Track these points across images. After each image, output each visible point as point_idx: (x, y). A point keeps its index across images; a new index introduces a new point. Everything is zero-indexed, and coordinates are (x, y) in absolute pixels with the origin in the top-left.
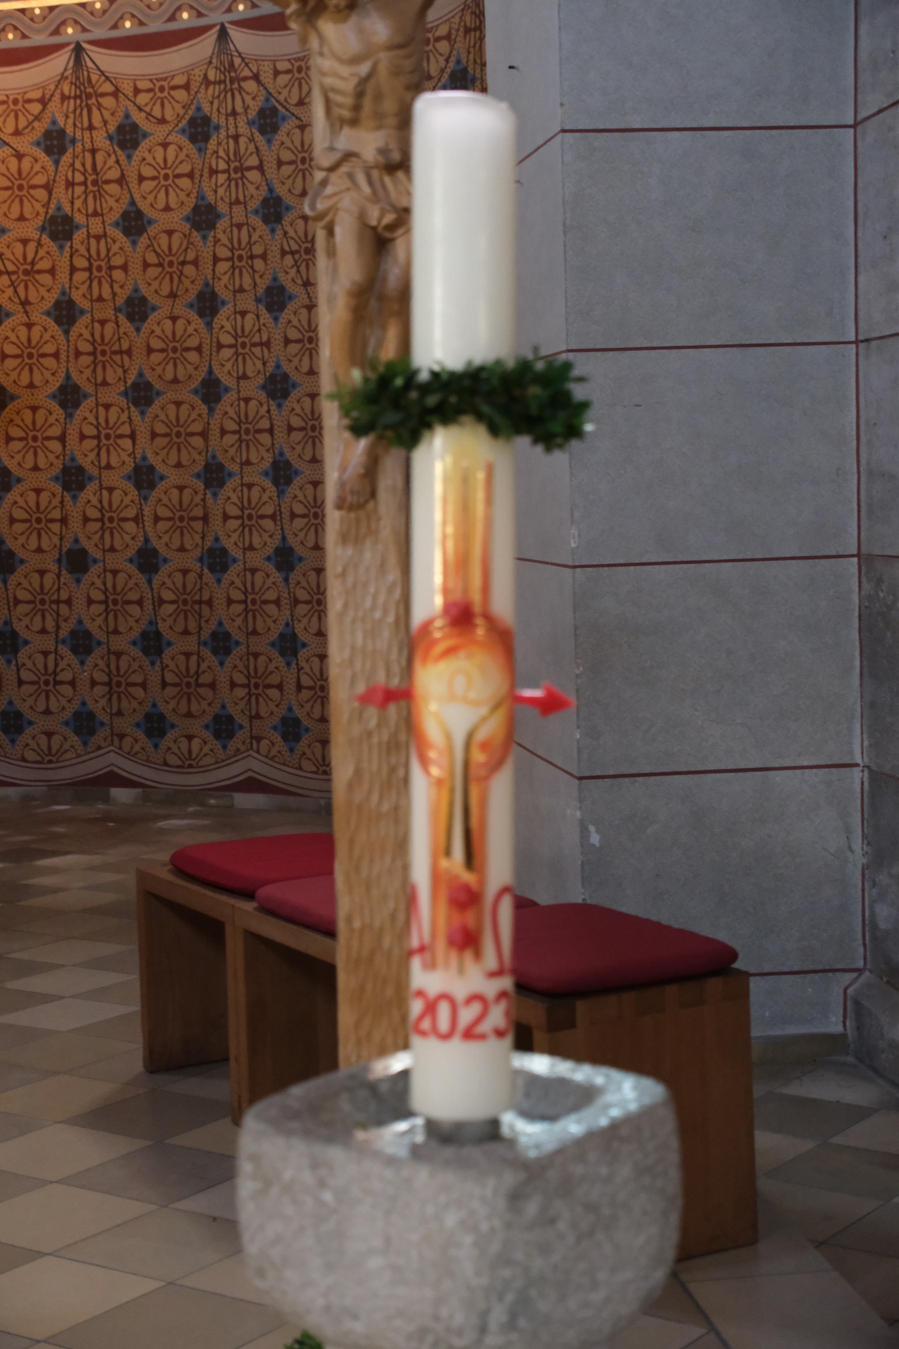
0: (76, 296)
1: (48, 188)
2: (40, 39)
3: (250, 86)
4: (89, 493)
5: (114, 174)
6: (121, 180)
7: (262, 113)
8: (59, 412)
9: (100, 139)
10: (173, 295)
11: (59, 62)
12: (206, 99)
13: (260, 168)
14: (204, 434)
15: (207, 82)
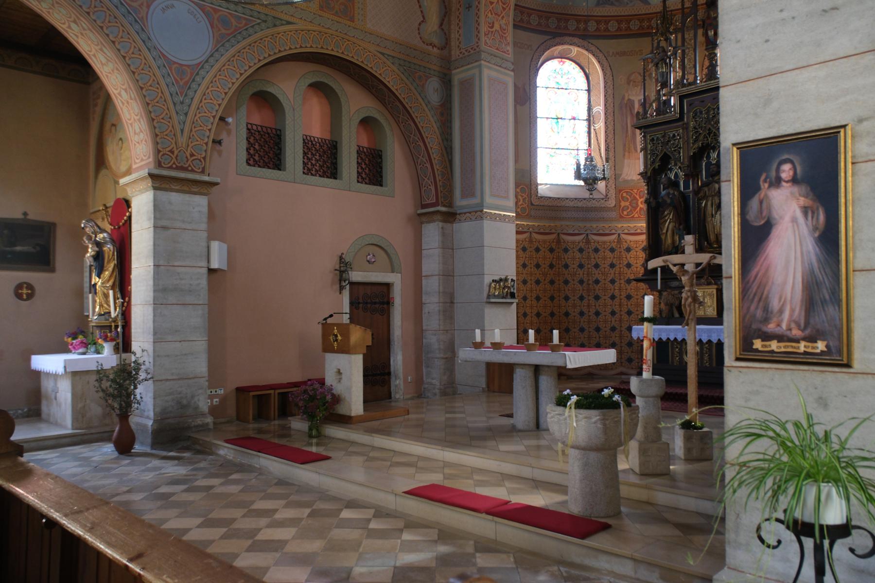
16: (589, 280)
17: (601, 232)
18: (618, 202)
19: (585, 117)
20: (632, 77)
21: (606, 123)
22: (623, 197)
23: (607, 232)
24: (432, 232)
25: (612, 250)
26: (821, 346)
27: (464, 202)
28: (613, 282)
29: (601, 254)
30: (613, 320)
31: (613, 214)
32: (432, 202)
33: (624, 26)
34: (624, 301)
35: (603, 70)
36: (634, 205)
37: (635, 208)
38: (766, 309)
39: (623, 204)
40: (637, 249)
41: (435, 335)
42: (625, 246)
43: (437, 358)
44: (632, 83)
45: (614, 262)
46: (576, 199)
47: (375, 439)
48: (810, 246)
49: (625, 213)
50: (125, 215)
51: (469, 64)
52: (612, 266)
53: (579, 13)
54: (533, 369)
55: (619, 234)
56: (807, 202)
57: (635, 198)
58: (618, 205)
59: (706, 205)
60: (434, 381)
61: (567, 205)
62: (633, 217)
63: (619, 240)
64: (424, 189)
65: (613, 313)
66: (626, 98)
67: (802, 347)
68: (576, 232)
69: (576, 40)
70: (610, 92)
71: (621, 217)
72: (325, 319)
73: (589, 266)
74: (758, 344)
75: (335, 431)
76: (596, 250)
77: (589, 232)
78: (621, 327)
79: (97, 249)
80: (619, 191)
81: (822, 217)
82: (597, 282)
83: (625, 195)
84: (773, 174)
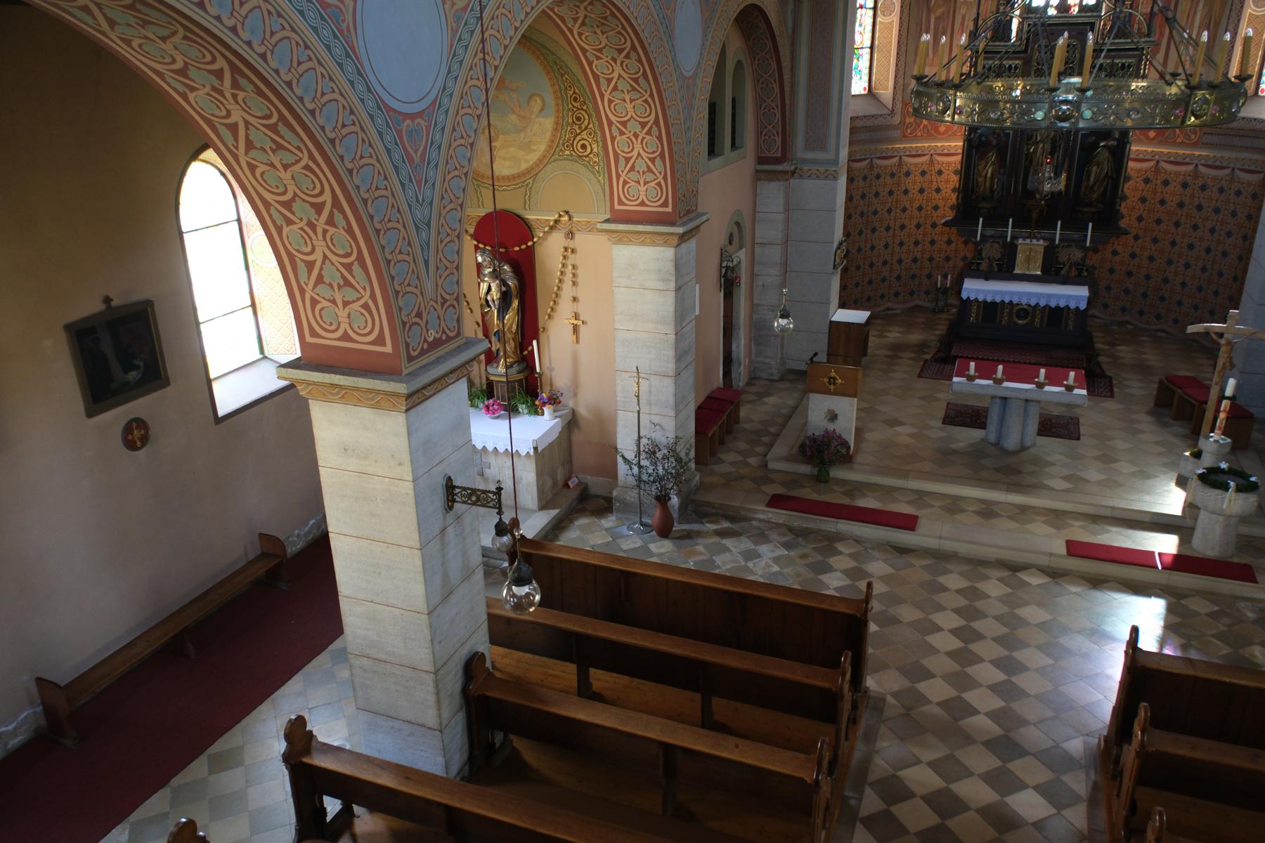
0: (1144, 216)
1: (1143, 191)
2: (1148, 157)
3: (1201, 179)
4: (1137, 260)
5: (1160, 190)
6: (1162, 192)
7: (1202, 186)
9: (1159, 182)
11: (1152, 164)
12: (1189, 179)
13: (1199, 198)
14: (1169, 253)
15: (1189, 175)
16: (868, 211)
17: (884, 155)
18: (903, 117)
21: (901, 18)
23: (890, 154)
24: (773, 193)
27: (809, 155)
28: (889, 211)
29: (882, 179)
30: (886, 252)
31: (897, 134)
37: (919, 125)
40: (916, 173)
41: (773, 311)
42: (905, 169)
46: (865, 117)
49: (909, 131)
52: (891, 193)
58: (903, 122)
59: (1035, 151)
60: (767, 360)
64: (763, 138)
68: (863, 157)
71: (905, 136)
72: (811, 359)
75: (838, 473)
76: (878, 177)
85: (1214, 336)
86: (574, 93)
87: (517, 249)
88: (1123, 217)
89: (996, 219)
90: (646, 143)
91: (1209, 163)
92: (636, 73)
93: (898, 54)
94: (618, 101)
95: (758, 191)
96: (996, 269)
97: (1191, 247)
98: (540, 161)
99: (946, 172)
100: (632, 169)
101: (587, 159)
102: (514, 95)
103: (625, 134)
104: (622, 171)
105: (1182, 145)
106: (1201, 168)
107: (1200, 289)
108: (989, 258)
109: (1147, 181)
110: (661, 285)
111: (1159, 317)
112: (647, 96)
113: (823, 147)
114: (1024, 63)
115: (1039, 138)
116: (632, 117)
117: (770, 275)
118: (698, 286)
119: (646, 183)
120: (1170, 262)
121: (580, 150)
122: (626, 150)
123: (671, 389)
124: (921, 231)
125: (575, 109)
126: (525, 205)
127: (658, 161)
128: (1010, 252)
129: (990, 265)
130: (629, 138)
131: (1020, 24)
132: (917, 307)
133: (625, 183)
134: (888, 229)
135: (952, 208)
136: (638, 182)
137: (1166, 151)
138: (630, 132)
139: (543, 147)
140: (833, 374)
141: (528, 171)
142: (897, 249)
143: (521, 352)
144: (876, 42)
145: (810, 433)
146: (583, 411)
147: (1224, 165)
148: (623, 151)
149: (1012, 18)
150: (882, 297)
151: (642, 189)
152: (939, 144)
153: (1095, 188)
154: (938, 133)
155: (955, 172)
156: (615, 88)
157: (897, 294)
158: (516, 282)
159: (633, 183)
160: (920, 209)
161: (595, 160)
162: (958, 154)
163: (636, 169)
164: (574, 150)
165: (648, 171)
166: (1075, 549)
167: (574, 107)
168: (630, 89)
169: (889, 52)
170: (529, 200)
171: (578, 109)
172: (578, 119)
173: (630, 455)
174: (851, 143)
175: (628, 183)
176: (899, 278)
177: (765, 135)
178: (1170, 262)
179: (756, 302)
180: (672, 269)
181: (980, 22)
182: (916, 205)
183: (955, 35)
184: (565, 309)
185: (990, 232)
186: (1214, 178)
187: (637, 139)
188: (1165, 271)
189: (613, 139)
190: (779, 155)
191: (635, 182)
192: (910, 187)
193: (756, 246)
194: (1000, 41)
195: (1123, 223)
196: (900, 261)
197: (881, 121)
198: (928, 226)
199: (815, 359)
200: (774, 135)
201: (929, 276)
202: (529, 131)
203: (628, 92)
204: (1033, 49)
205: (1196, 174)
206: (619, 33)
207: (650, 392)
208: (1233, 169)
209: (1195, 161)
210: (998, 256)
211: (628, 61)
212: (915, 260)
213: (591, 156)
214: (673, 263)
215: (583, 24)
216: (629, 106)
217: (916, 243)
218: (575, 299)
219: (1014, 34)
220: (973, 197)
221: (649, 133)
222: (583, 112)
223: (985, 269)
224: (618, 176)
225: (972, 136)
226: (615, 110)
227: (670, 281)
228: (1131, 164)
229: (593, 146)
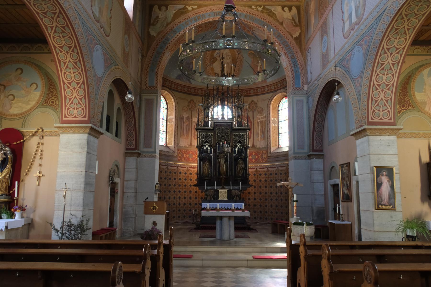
1: (254, 178)
2: (254, 168)
4: (256, 200)
6: (259, 178)
8: (254, 194)
10: (263, 186)
11: (255, 169)
12: (266, 173)
16: (167, 184)
17: (172, 165)
19: (166, 119)
20: (184, 108)
22: (179, 153)
23: (174, 165)
24: (132, 161)
25: (175, 173)
26: (391, 206)
27: (145, 150)
28: (175, 185)
30: (174, 200)
31: (176, 159)
32: (132, 148)
33: (183, 89)
34: (178, 193)
35: (175, 103)
36: (183, 156)
38: (382, 199)
39: (179, 155)
40: (183, 173)
41: (131, 207)
43: (131, 217)
44: (184, 110)
45: (176, 178)
46: (165, 151)
47: (188, 248)
48: (389, 188)
49: (180, 159)
50: (20, 141)
51: (151, 93)
52: (175, 179)
53: (170, 80)
54: (228, 217)
55: (178, 167)
56: (389, 180)
57: (183, 154)
58: (177, 156)
59: (220, 161)
60: (129, 228)
61: (162, 153)
62: (182, 161)
63: (178, 169)
65: (174, 198)
66: (182, 115)
67: (388, 207)
68: (164, 164)
69: (168, 89)
70: (177, 112)
71: (179, 160)
72: (146, 200)
73: (168, 179)
74: (380, 206)
76: (170, 172)
77: (168, 165)
78: (177, 203)
79: (4, 157)
80: (178, 150)
81: (391, 183)
82: (170, 185)
83: (180, 152)
84: (382, 173)
85: (286, 186)
86: (51, 82)
87: (15, 143)
88: (250, 181)
89: (210, 183)
90: (79, 92)
91: (271, 167)
92: (76, 60)
93: (175, 134)
94: (68, 73)
95: (126, 161)
96: (213, 199)
97: (271, 193)
98: (32, 108)
99: (193, 174)
100: (72, 103)
101: (54, 107)
102: (25, 83)
103: (70, 88)
104: (68, 104)
105: (262, 163)
106: (269, 169)
107: (277, 206)
108: (210, 195)
109: (255, 175)
110: (80, 150)
111: (266, 219)
112: (80, 71)
113: (150, 147)
114: (214, 133)
115: (221, 157)
116: (73, 80)
117: (130, 193)
118: (97, 162)
119: (77, 109)
120: (266, 199)
121: (51, 104)
122: (70, 95)
123: (82, 197)
124: (186, 193)
125: (50, 88)
126: (22, 125)
127: (83, 99)
128: (217, 191)
129: (211, 198)
130: (71, 90)
131: (212, 122)
132: (187, 222)
133: (68, 109)
134: (175, 192)
135: (196, 180)
136: (74, 109)
137: (258, 165)
138: (72, 87)
139: (34, 103)
140: (154, 205)
141: (26, 112)
142: (178, 199)
143: (9, 192)
144: (168, 131)
145: (145, 230)
146: (37, 219)
147: (275, 166)
148: (68, 96)
149: (209, 121)
150: (174, 217)
151: (76, 111)
152: (190, 164)
153: (240, 172)
154: (189, 160)
155: (196, 174)
156: (67, 67)
157: (179, 217)
158: (11, 156)
159: (72, 109)
160: (185, 186)
161: (56, 107)
162: (196, 168)
163: (73, 103)
164: (48, 104)
165: (78, 104)
166: (255, 259)
167: (50, 88)
168: (73, 67)
169: (172, 133)
170: (25, 124)
171: (52, 88)
172: (52, 92)
173: (58, 226)
174: (160, 159)
175: (70, 109)
176: (179, 210)
177: (129, 140)
178: (266, 199)
179: (124, 204)
180: (87, 143)
181: (200, 122)
182: (184, 184)
183: (192, 131)
184: (35, 172)
185: (209, 188)
186: (273, 171)
187: (75, 90)
188: (265, 203)
189: (65, 90)
190: (134, 148)
191: (73, 108)
192: (181, 178)
193: (125, 181)
194: (206, 127)
195: (250, 183)
196: (179, 204)
197: (170, 154)
198: (188, 192)
199: (147, 200)
200: (132, 140)
201: (190, 210)
202: (29, 96)
203: (73, 69)
204: (216, 129)
205: (268, 171)
206: (70, 37)
207: (71, 199)
208: (278, 167)
209: (267, 167)
210: (213, 194)
211: (73, 53)
212: (185, 204)
213: (55, 106)
214: (87, 141)
215: (55, 31)
216: (73, 75)
217: (185, 198)
218: (40, 165)
219: (210, 125)
220: (203, 177)
221: (80, 87)
222: (54, 90)
223: (209, 199)
224: (66, 106)
225: (200, 155)
226: (66, 77)
227: (84, 148)
228: (249, 170)
229: (57, 102)
